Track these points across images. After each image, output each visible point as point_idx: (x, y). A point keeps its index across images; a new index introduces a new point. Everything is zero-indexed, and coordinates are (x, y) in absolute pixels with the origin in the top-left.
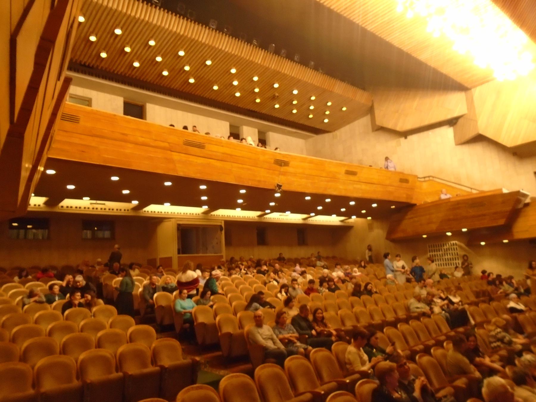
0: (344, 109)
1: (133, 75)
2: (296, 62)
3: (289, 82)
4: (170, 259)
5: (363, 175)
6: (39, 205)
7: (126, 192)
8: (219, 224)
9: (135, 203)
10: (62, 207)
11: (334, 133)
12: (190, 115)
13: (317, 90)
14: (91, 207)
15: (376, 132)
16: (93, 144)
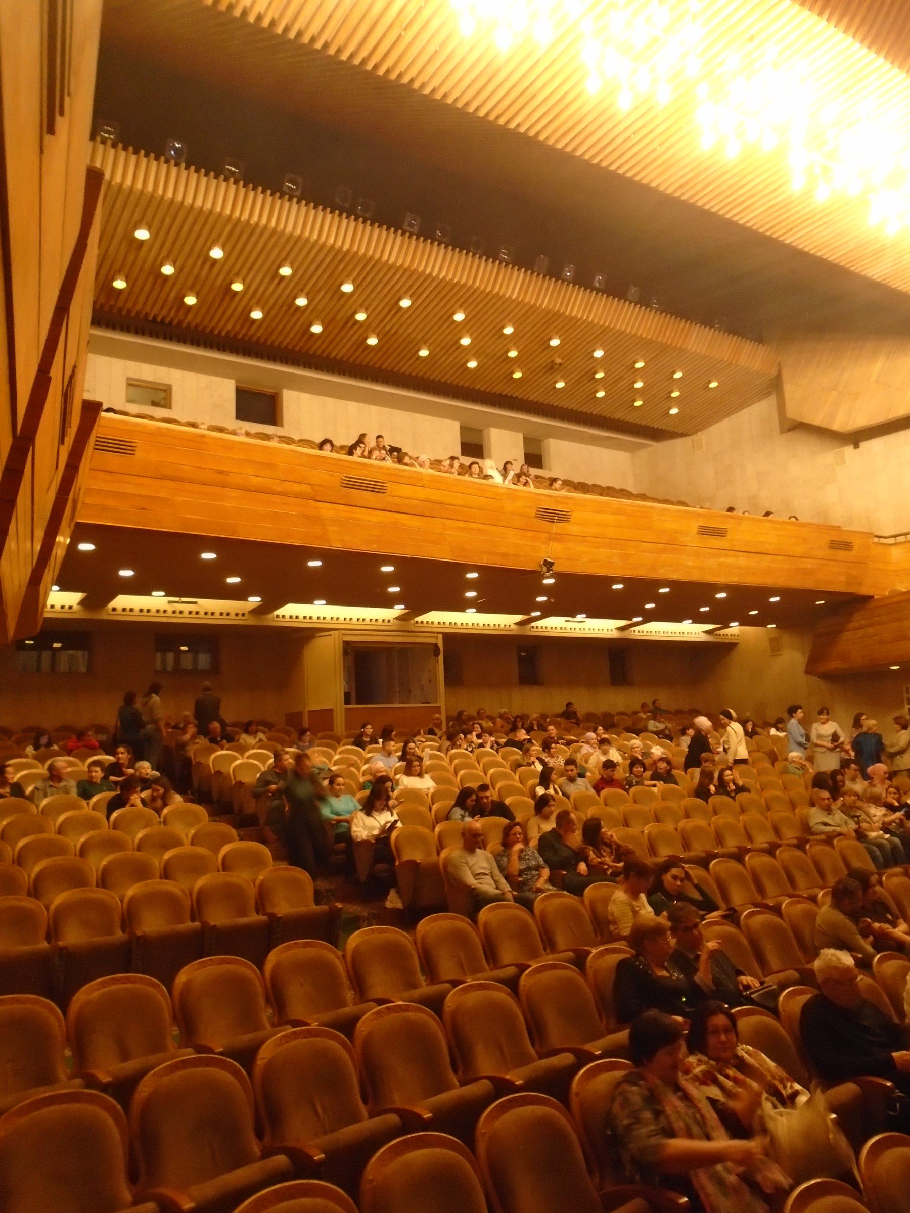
0: (713, 385)
1: (252, 336)
2: (598, 290)
3: (582, 336)
4: (327, 714)
5: (742, 533)
6: (70, 607)
7: (233, 580)
8: (433, 641)
9: (255, 600)
10: (114, 609)
11: (695, 437)
12: (374, 409)
13: (644, 345)
14: (170, 608)
15: (790, 433)
16: (163, 494)
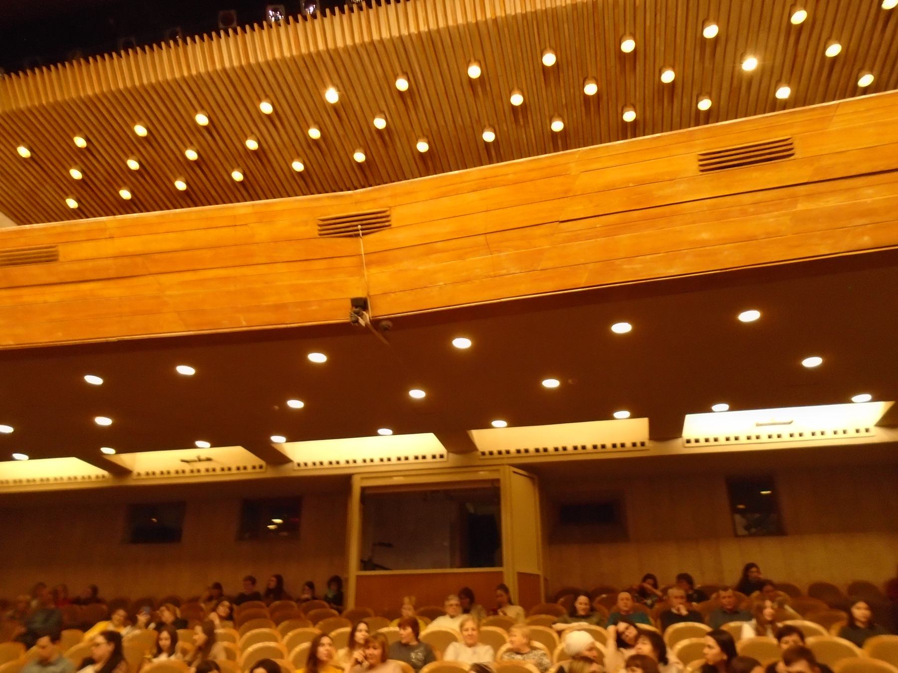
14: (188, 468)
